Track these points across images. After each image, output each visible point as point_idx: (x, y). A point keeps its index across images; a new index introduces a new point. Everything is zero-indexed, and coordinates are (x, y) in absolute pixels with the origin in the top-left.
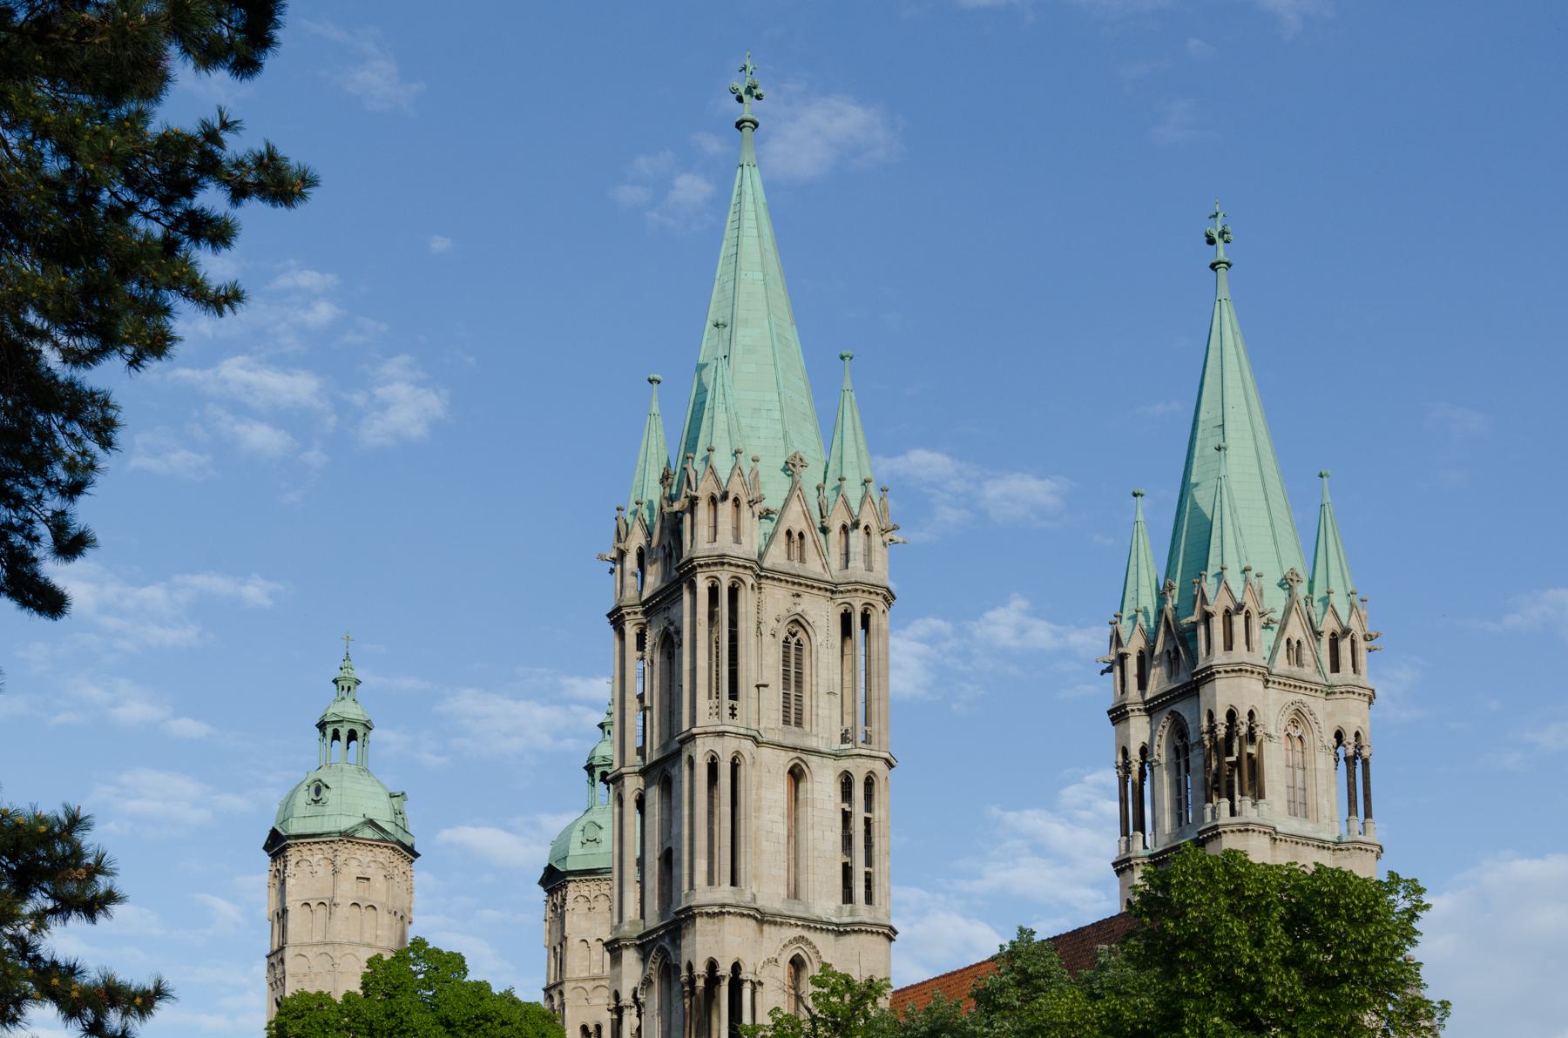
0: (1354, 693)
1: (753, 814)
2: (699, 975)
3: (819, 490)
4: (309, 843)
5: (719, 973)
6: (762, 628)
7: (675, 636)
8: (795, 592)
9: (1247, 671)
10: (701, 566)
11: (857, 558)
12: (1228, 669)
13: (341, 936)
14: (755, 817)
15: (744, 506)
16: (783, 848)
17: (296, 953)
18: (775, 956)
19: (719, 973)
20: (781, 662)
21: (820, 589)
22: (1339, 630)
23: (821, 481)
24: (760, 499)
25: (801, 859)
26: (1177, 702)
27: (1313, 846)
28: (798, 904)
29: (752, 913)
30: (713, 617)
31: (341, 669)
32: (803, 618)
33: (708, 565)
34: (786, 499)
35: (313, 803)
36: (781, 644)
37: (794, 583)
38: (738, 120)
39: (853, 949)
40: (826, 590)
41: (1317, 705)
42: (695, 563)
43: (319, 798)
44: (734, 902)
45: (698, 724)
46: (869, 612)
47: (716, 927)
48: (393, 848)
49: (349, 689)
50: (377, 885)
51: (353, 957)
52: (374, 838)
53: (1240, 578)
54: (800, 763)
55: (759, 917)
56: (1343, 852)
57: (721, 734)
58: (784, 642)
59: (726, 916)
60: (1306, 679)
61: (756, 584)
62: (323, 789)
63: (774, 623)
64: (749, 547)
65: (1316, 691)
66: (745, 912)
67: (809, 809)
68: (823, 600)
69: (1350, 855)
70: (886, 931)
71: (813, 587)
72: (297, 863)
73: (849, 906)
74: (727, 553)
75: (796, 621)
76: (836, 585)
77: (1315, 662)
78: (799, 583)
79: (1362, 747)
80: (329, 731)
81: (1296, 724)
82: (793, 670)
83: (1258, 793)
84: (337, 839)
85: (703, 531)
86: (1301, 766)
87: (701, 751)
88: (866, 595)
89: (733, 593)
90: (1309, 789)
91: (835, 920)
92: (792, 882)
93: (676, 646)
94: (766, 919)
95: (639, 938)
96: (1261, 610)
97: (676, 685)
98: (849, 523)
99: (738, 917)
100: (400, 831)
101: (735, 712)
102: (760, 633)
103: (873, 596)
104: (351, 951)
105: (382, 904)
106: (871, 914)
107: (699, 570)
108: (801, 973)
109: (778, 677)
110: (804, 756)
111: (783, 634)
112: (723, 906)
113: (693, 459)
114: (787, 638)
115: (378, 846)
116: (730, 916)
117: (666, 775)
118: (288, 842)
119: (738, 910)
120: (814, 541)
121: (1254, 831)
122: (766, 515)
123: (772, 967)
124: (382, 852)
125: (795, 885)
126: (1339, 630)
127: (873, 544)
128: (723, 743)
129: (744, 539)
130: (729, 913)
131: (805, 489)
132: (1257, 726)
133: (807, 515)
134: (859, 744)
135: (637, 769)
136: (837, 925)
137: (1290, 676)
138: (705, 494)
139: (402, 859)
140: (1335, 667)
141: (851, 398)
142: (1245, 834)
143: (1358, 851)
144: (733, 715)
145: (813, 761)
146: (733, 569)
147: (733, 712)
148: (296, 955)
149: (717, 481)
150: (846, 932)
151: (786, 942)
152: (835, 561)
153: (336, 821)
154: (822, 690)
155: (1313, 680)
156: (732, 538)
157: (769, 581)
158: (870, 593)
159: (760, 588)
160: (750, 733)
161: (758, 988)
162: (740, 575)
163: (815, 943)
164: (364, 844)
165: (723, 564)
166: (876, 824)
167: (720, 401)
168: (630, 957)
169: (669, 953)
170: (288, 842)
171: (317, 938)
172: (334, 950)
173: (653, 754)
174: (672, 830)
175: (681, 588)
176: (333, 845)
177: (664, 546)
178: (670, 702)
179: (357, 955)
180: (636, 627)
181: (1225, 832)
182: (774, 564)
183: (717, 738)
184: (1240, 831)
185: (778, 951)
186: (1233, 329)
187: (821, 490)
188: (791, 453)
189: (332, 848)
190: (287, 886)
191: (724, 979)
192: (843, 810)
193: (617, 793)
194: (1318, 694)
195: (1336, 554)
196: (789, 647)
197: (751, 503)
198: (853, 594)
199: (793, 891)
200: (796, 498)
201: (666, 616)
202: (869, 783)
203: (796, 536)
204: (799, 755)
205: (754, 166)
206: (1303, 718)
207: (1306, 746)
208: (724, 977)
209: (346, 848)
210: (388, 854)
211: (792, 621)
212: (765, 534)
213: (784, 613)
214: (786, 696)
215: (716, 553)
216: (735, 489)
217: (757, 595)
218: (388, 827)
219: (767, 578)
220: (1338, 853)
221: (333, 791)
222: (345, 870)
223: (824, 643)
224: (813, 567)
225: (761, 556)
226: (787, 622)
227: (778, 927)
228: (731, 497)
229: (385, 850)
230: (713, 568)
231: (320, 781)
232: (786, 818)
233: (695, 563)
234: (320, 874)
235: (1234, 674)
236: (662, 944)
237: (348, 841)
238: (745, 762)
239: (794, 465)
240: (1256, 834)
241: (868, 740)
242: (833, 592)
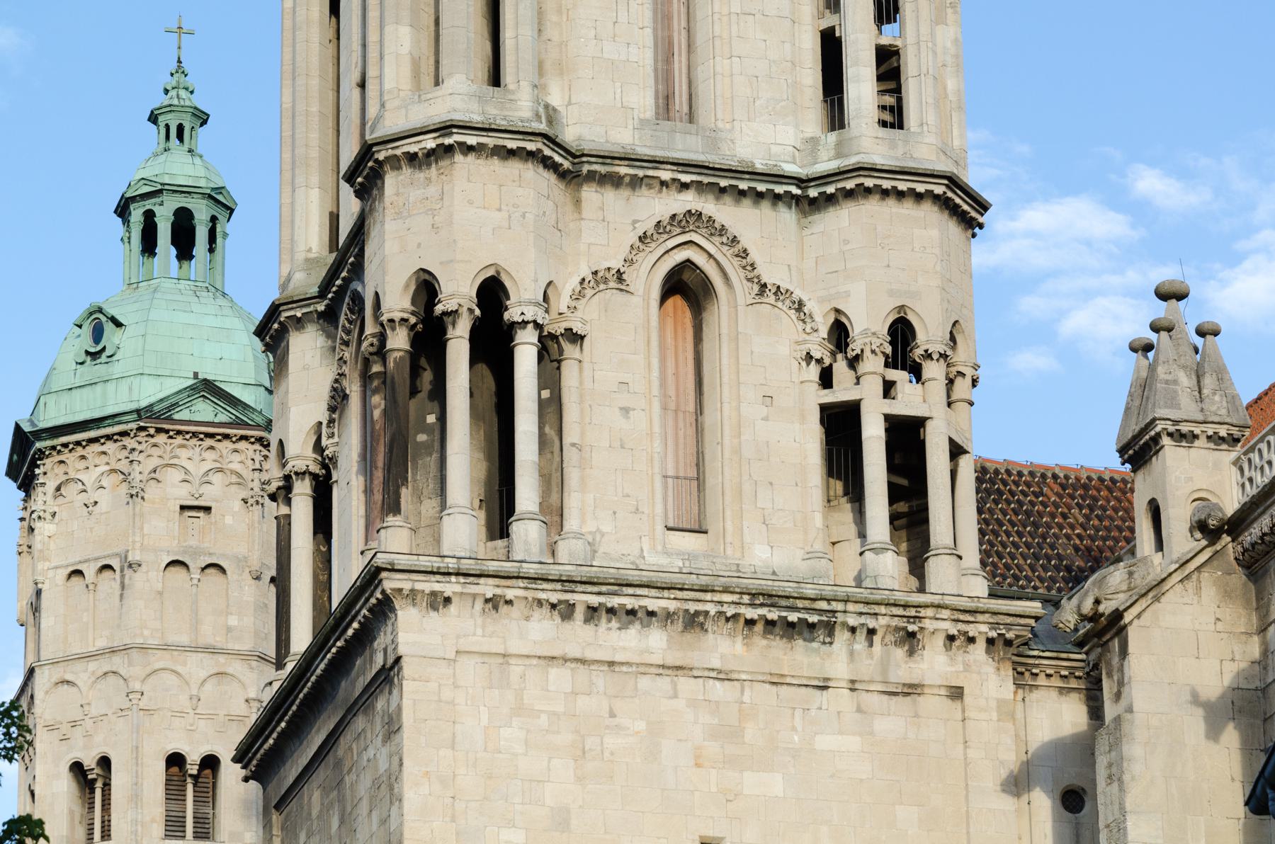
2: (391, 321)
4: (78, 443)
13: (146, 633)
17: (54, 679)
18: (616, 264)
19: (439, 309)
29: (531, 146)
31: (166, 91)
35: (89, 358)
39: (846, 242)
43: (99, 348)
44: (476, 118)
47: (433, 190)
50: (229, 520)
51: (173, 677)
52: (216, 420)
55: (566, 164)
62: (108, 327)
66: (512, 145)
70: (939, 190)
72: (58, 489)
73: (833, 137)
84: (134, 426)
91: (791, 169)
94: (586, 168)
99: (495, 162)
104: (169, 664)
105: (241, 561)
106: (893, 145)
108: (705, 315)
112: (445, 128)
115: (226, 437)
116: (471, 158)
118: (38, 445)
119: (490, 141)
123: (610, 296)
124: (236, 451)
125: (690, 95)
136: (801, 182)
150: (830, 200)
151: (649, 226)
153: (130, 389)
161: (570, 350)
163: (733, 229)
164: (195, 434)
170: (38, 445)
172: (130, 664)
176: (127, 441)
179: (179, 669)
185: (624, 252)
189: (124, 447)
191: (454, 325)
199: (685, 109)
210: (250, 454)
221: (129, 331)
222: (152, 491)
227: (625, 192)
229: (243, 445)
231: (100, 310)
234: (103, 506)
237: (159, 430)
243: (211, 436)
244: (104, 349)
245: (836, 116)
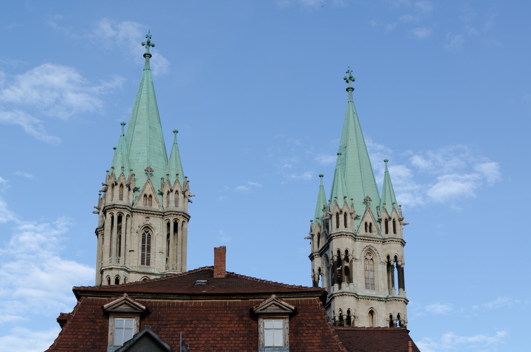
0: (393, 241)
9: (344, 235)
10: (108, 209)
12: (337, 235)
15: (125, 187)
22: (388, 218)
26: (327, 250)
27: (376, 300)
33: (110, 209)
40: (160, 215)
41: (378, 247)
46: (177, 222)
53: (343, 201)
56: (389, 302)
57: (111, 269)
58: (143, 235)
60: (372, 237)
63: (138, 229)
65: (378, 241)
69: (392, 302)
74: (115, 204)
75: (147, 227)
76: (164, 213)
77: (377, 230)
78: (148, 213)
79: (398, 261)
81: (370, 254)
83: (350, 281)
86: (372, 270)
88: (175, 216)
90: (375, 279)
96: (351, 212)
103: (178, 216)
107: (107, 211)
114: (144, 233)
120: (155, 198)
121: (346, 295)
122: (136, 190)
126: (388, 218)
128: (112, 272)
132: (349, 255)
133: (153, 189)
137: (365, 236)
138: (110, 183)
140: (387, 232)
142: (343, 296)
143: (395, 301)
146: (119, 209)
152: (165, 206)
155: (376, 237)
156: (119, 198)
157: (136, 213)
158: (177, 215)
159: (132, 216)
162: (122, 211)
165: (115, 208)
167: (120, 151)
181: (336, 296)
182: (138, 207)
183: (110, 271)
184: (341, 295)
186: (353, 111)
194: (379, 242)
195: (389, 189)
198: (170, 216)
203: (148, 196)
204: (146, 275)
206: (373, 252)
207: (374, 262)
214: (143, 255)
215: (112, 204)
219: (135, 212)
220: (388, 302)
224: (155, 207)
226: (143, 228)
228: (119, 184)
235: (339, 237)
240: (347, 296)
242: (163, 216)
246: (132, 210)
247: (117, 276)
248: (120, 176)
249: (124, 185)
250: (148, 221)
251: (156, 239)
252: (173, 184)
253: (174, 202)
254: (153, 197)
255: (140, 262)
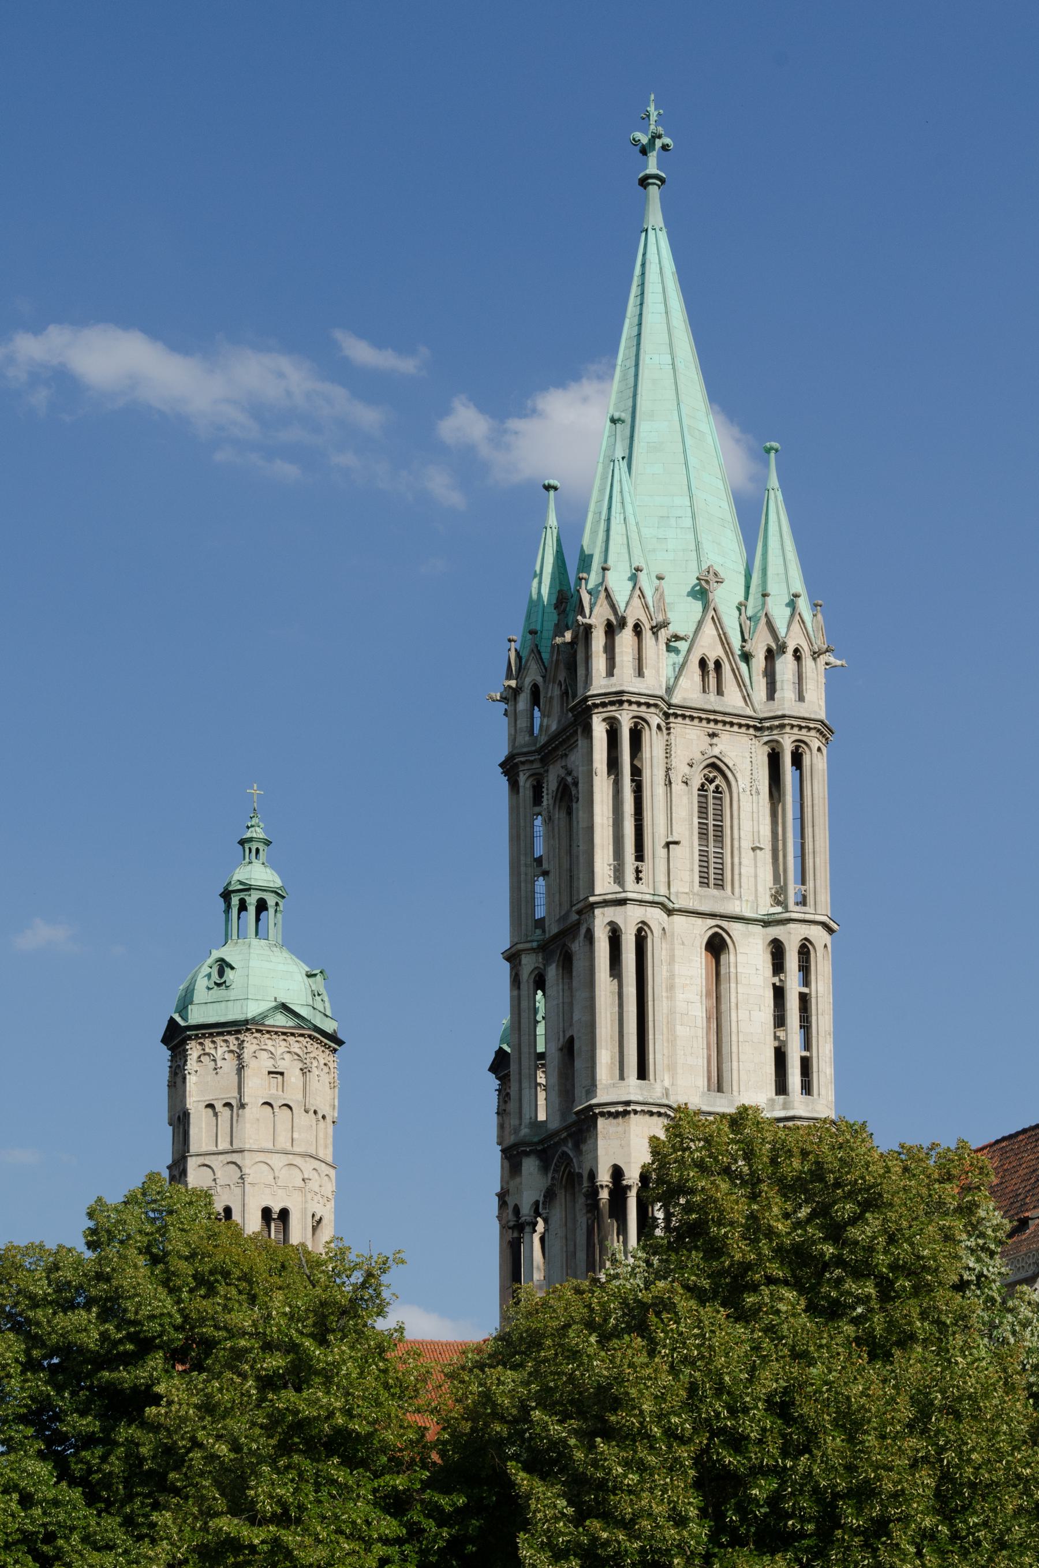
1: (664, 994)
2: (602, 1186)
3: (739, 610)
5: (625, 1183)
6: (672, 776)
7: (573, 789)
8: (711, 731)
10: (596, 706)
11: (785, 687)
13: (251, 1141)
14: (667, 997)
15: (647, 634)
16: (701, 1033)
19: (625, 1183)
20: (696, 814)
21: (740, 726)
23: (742, 599)
24: (665, 625)
25: (724, 1045)
28: (722, 1098)
29: (662, 1110)
30: (613, 764)
32: (722, 761)
33: (604, 705)
34: (699, 622)
36: (696, 792)
37: (709, 721)
38: (641, 175)
40: (748, 727)
42: (590, 703)
44: (640, 1099)
45: (597, 892)
47: (620, 1129)
48: (310, 1036)
49: (257, 850)
54: (720, 931)
55: (672, 1115)
57: (622, 902)
59: (632, 1115)
61: (663, 724)
64: (653, 683)
66: (655, 1110)
67: (733, 985)
68: (745, 739)
71: (732, 724)
75: (713, 766)
76: (762, 720)
80: (235, 901)
82: (711, 822)
85: (599, 662)
87: (601, 919)
89: (636, 736)
92: (714, 1074)
93: (575, 800)
95: (541, 1142)
97: (575, 845)
98: (774, 646)
99: (647, 1117)
100: (319, 1016)
101: (641, 875)
102: (669, 783)
103: (804, 731)
106: (807, 1105)
109: (692, 833)
110: (724, 924)
111: (697, 781)
112: (628, 1103)
113: (587, 580)
114: (703, 785)
117: (567, 951)
119: (646, 1108)
127: (804, 670)
129: (646, 672)
130: (635, 1112)
131: (721, 609)
133: (724, 640)
134: (792, 906)
135: (535, 944)
139: (323, 1048)
141: (776, 497)
144: (638, 879)
145: (736, 929)
147: (637, 875)
148: (228, 1163)
149: (613, 607)
153: (242, 1007)
154: (746, 844)
156: (632, 671)
157: (680, 720)
159: (668, 729)
160: (657, 899)
162: (643, 715)
164: (276, 1033)
166: (813, 1001)
168: (530, 1166)
169: (572, 1160)
171: (224, 1145)
173: (553, 929)
174: (574, 1015)
175: (576, 732)
177: (560, 681)
178: (570, 865)
180: (531, 779)
182: (685, 699)
187: (743, 608)
188: (705, 567)
190: (188, 1084)
192: (774, 985)
193: (513, 974)
196: (706, 796)
197: (655, 630)
199: (716, 1082)
200: (710, 620)
201: (563, 764)
202: (805, 951)
203: (711, 665)
204: (719, 922)
205: (661, 230)
208: (629, 1187)
209: (255, 1038)
210: (305, 1044)
211: (707, 766)
212: (674, 664)
213: (698, 756)
214: (704, 855)
215: (614, 690)
216: (634, 614)
217: (666, 737)
218: (303, 1012)
219: (676, 716)
223: (748, 789)
224: (733, 700)
225: (670, 690)
226: (702, 767)
228: (630, 623)
229: (301, 1039)
230: (610, 708)
232: (704, 997)
233: (590, 703)
236: (565, 1149)
238: (652, 932)
239: (707, 582)
241: (803, 902)
243: (284, 1034)
244: (225, 982)
245: (781, 1087)
246: (669, 709)
247: (640, 925)
248: (631, 596)
249: (646, 626)
250: (714, 746)
251: (741, 804)
252: (786, 626)
253: (791, 686)
254: (726, 668)
255: (697, 879)
